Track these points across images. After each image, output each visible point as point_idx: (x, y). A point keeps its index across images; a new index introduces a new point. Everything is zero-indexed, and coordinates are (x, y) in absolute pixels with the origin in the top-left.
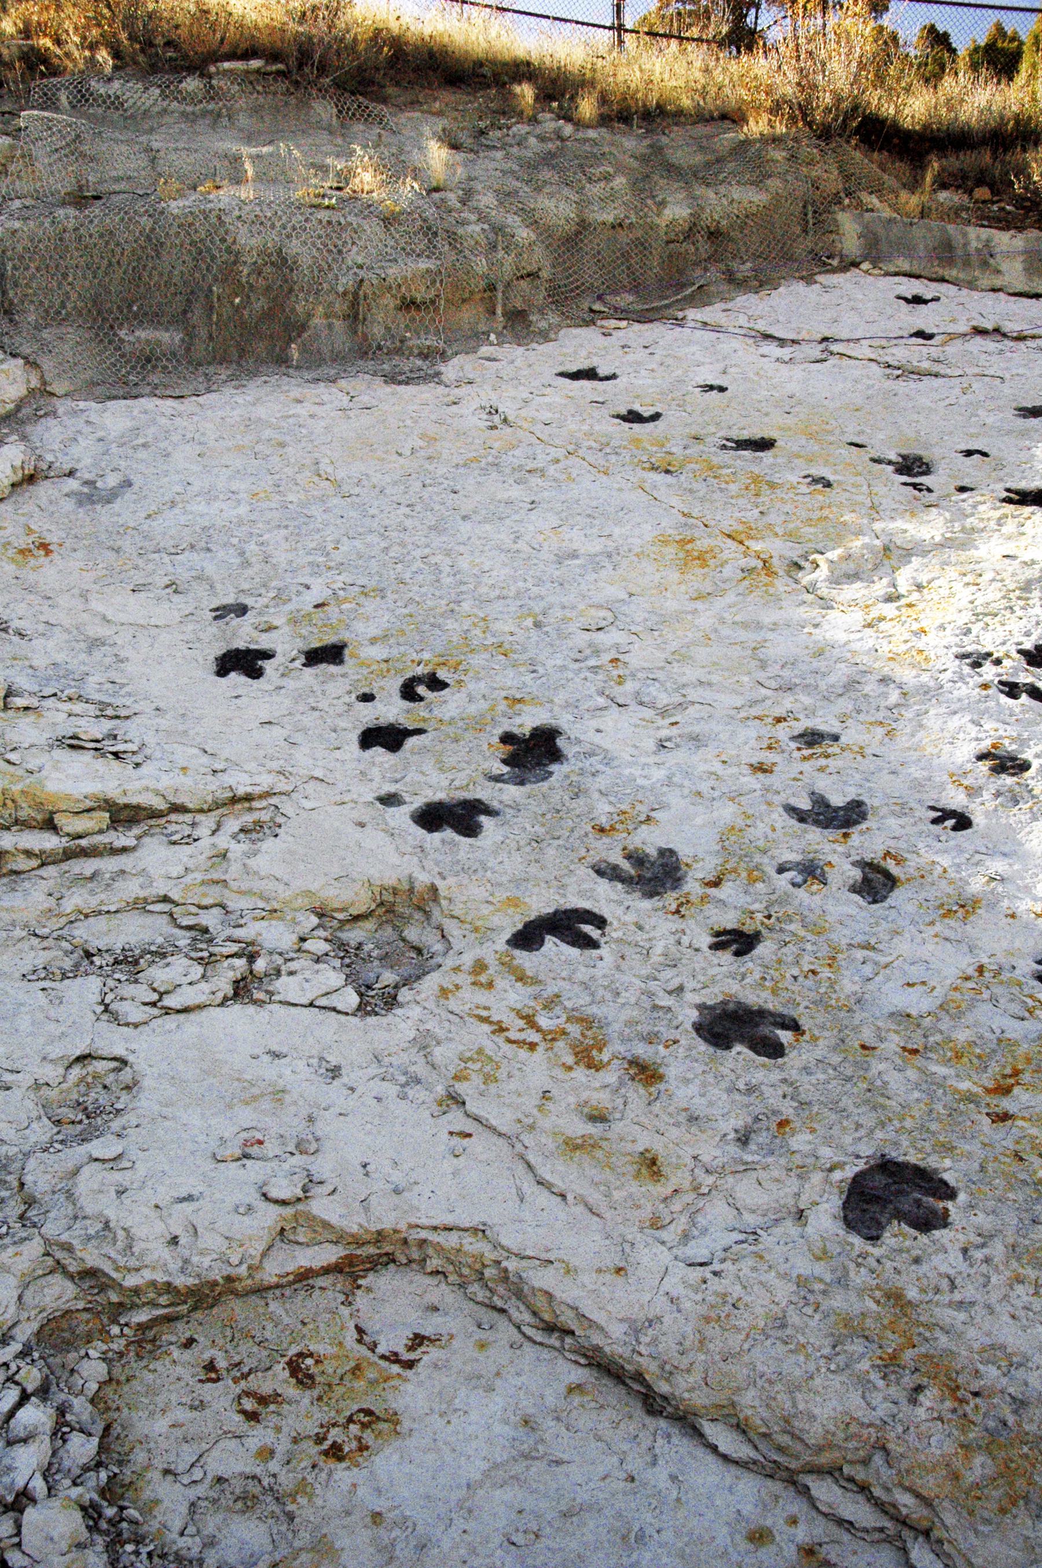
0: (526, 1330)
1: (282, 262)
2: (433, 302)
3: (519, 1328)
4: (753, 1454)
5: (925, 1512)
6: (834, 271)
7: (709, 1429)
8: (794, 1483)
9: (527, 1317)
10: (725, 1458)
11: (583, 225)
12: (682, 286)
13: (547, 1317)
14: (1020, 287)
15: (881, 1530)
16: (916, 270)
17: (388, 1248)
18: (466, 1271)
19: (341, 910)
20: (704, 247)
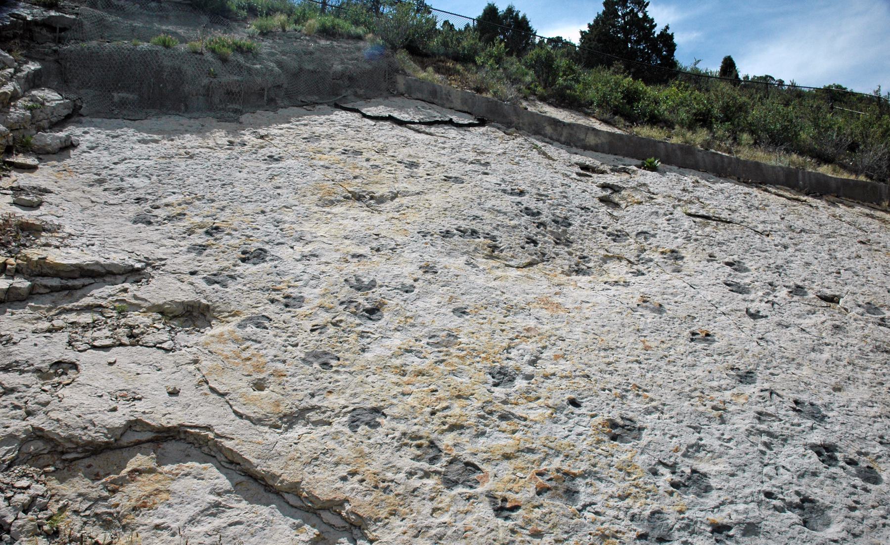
0: (223, 463)
1: (179, 71)
2: (239, 92)
3: (220, 462)
4: (302, 504)
5: (360, 520)
6: (394, 96)
7: (286, 496)
8: (316, 513)
9: (224, 459)
10: (292, 506)
11: (301, 69)
12: (337, 95)
13: (230, 458)
14: (459, 108)
15: (344, 527)
16: (424, 99)
17: (172, 434)
18: (201, 442)
19: (172, 313)
20: (347, 83)
